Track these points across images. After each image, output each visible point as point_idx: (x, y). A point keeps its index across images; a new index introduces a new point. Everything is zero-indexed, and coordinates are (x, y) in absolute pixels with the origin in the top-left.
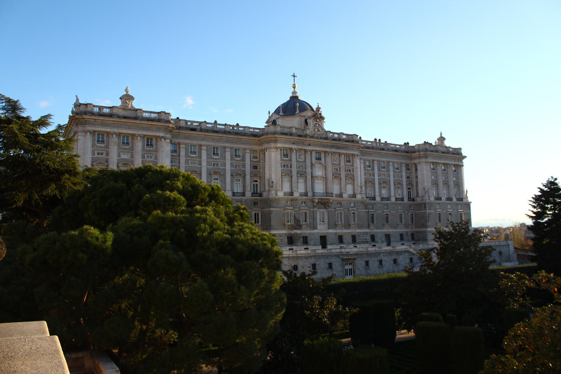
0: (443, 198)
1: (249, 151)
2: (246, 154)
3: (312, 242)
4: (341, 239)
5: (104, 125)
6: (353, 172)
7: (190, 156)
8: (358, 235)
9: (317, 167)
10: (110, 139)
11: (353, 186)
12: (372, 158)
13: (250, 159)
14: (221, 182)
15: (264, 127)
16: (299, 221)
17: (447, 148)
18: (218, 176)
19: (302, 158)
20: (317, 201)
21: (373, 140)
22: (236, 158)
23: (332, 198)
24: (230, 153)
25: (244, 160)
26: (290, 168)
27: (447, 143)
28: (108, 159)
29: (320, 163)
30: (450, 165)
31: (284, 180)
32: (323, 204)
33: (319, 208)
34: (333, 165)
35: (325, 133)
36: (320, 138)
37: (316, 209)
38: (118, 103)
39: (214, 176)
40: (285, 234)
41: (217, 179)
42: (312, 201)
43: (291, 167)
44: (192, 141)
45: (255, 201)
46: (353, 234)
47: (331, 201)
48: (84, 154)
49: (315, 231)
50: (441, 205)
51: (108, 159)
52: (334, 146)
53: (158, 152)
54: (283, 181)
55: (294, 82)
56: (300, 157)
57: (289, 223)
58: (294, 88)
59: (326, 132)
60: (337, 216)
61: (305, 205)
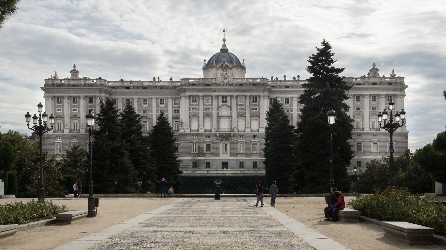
0: (367, 129)
1: (171, 100)
2: (169, 102)
3: (214, 167)
4: (242, 165)
5: (59, 91)
6: (259, 110)
8: (260, 162)
9: (223, 108)
11: (258, 122)
12: (291, 96)
13: (171, 106)
14: (149, 124)
15: (180, 81)
16: (203, 151)
17: (380, 79)
19: (209, 102)
20: (218, 135)
21: (292, 80)
23: (233, 132)
25: (167, 106)
26: (198, 111)
28: (64, 113)
29: (226, 105)
30: (381, 96)
31: (193, 120)
32: (226, 137)
33: (223, 141)
34: (239, 106)
35: (232, 80)
36: (226, 85)
37: (219, 141)
38: (69, 76)
39: (143, 119)
40: (191, 160)
41: (146, 122)
42: (215, 134)
43: (199, 110)
44: (126, 96)
46: (254, 161)
47: (232, 135)
49: (217, 158)
50: (362, 135)
51: (64, 113)
52: (239, 90)
54: (192, 121)
56: (208, 101)
57: (195, 152)
60: (238, 146)
61: (209, 138)
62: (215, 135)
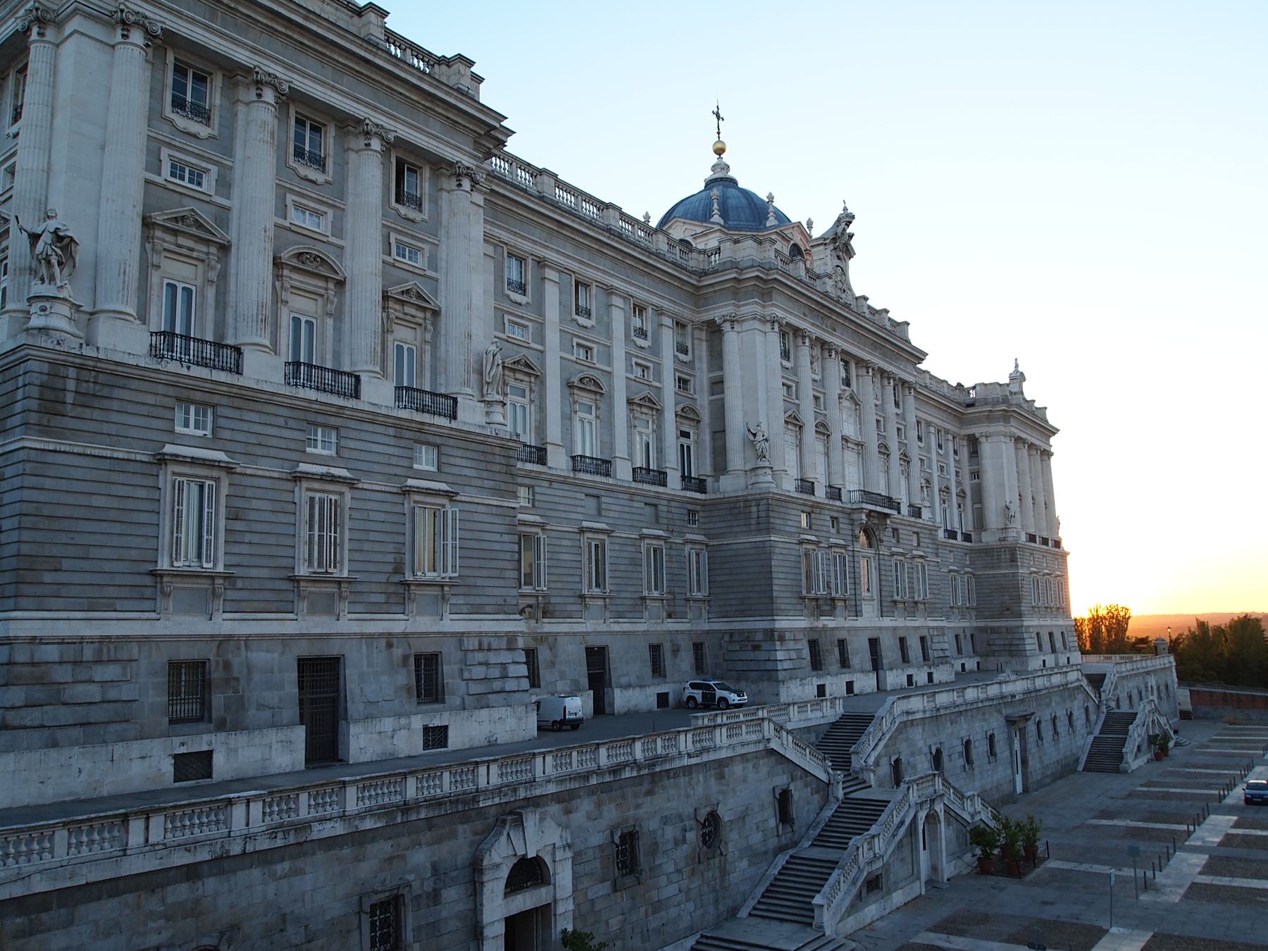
2: (664, 329)
7: (508, 296)
10: (241, 108)
18: (593, 397)
22: (635, 339)
24: (622, 312)
25: (655, 350)
27: (1029, 391)
28: (229, 209)
44: (515, 234)
45: (690, 507)
48: (103, 148)
49: (860, 622)
53: (443, 239)
55: (719, 133)
58: (720, 151)
59: (857, 298)
62: (846, 516)
